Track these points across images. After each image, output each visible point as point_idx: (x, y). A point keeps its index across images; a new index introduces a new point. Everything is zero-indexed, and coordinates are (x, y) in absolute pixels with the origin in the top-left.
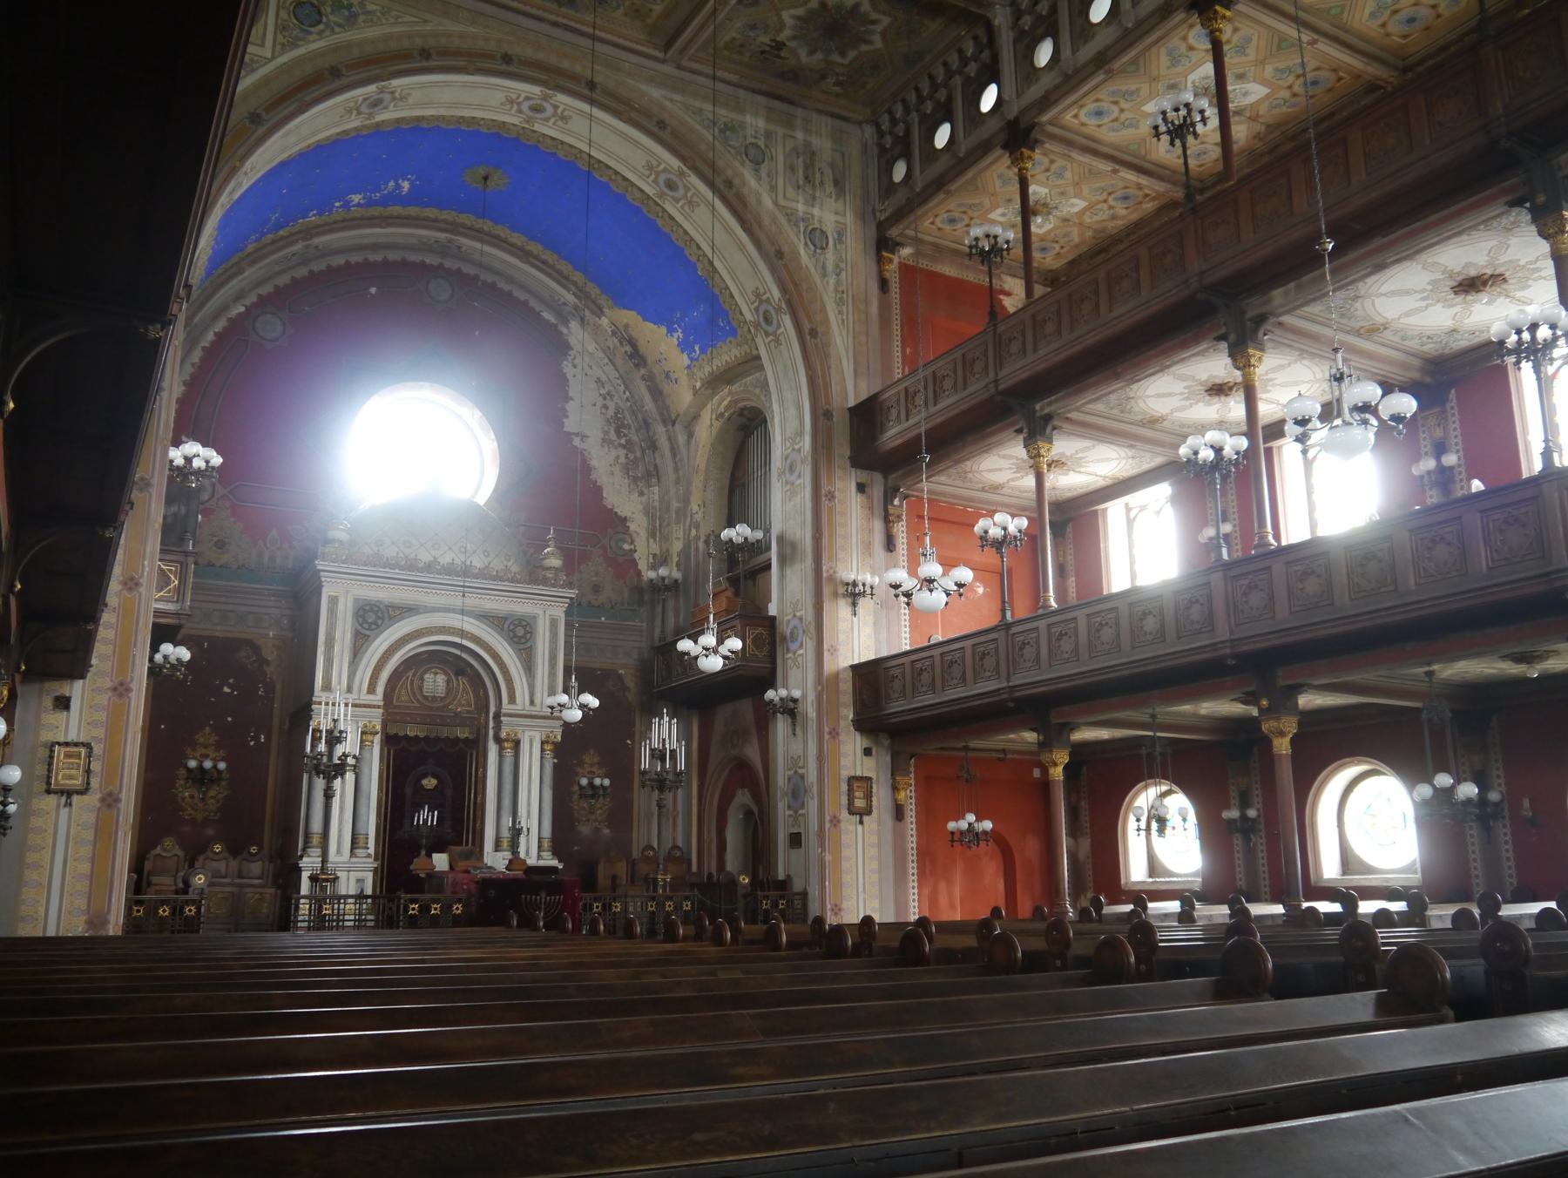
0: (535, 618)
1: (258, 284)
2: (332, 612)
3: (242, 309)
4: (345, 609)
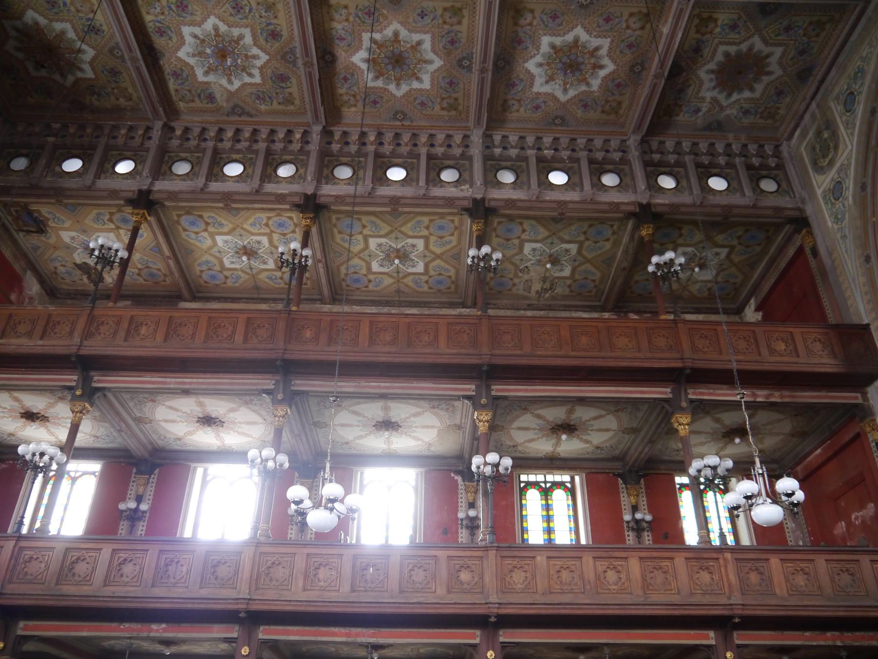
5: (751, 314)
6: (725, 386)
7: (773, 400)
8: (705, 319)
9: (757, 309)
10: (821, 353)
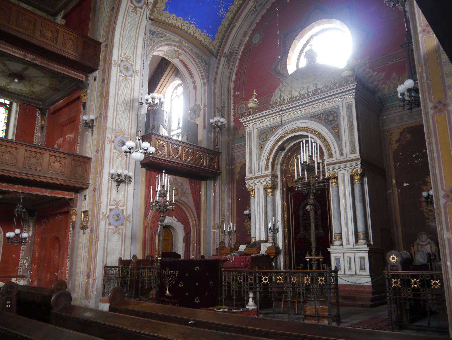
0: (338, 108)
1: (250, 26)
2: (250, 138)
3: (248, 38)
4: (255, 135)
5: (60, 20)
6: (8, 44)
7: (35, 62)
8: (32, 11)
9: (63, 18)
10: (70, 47)
